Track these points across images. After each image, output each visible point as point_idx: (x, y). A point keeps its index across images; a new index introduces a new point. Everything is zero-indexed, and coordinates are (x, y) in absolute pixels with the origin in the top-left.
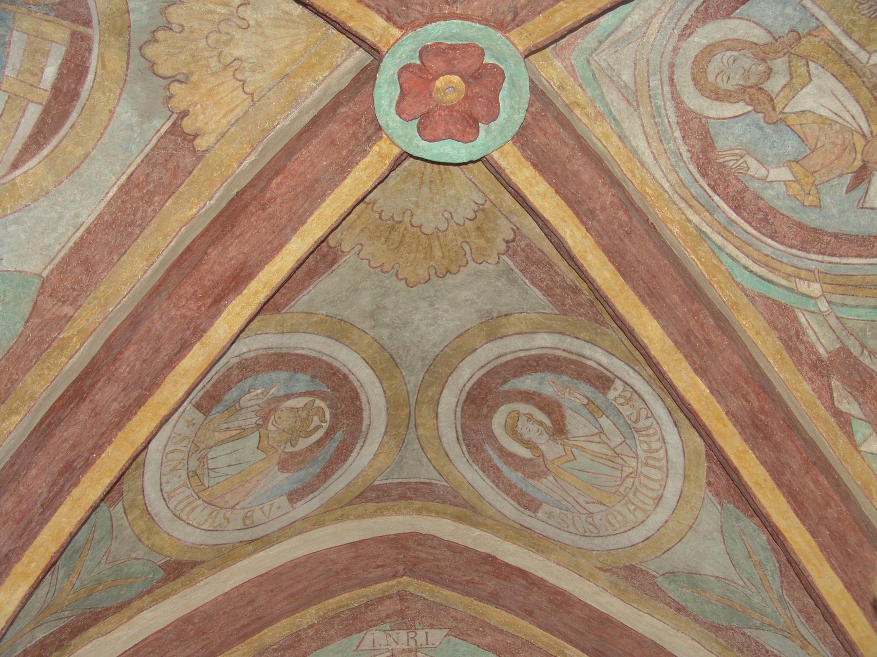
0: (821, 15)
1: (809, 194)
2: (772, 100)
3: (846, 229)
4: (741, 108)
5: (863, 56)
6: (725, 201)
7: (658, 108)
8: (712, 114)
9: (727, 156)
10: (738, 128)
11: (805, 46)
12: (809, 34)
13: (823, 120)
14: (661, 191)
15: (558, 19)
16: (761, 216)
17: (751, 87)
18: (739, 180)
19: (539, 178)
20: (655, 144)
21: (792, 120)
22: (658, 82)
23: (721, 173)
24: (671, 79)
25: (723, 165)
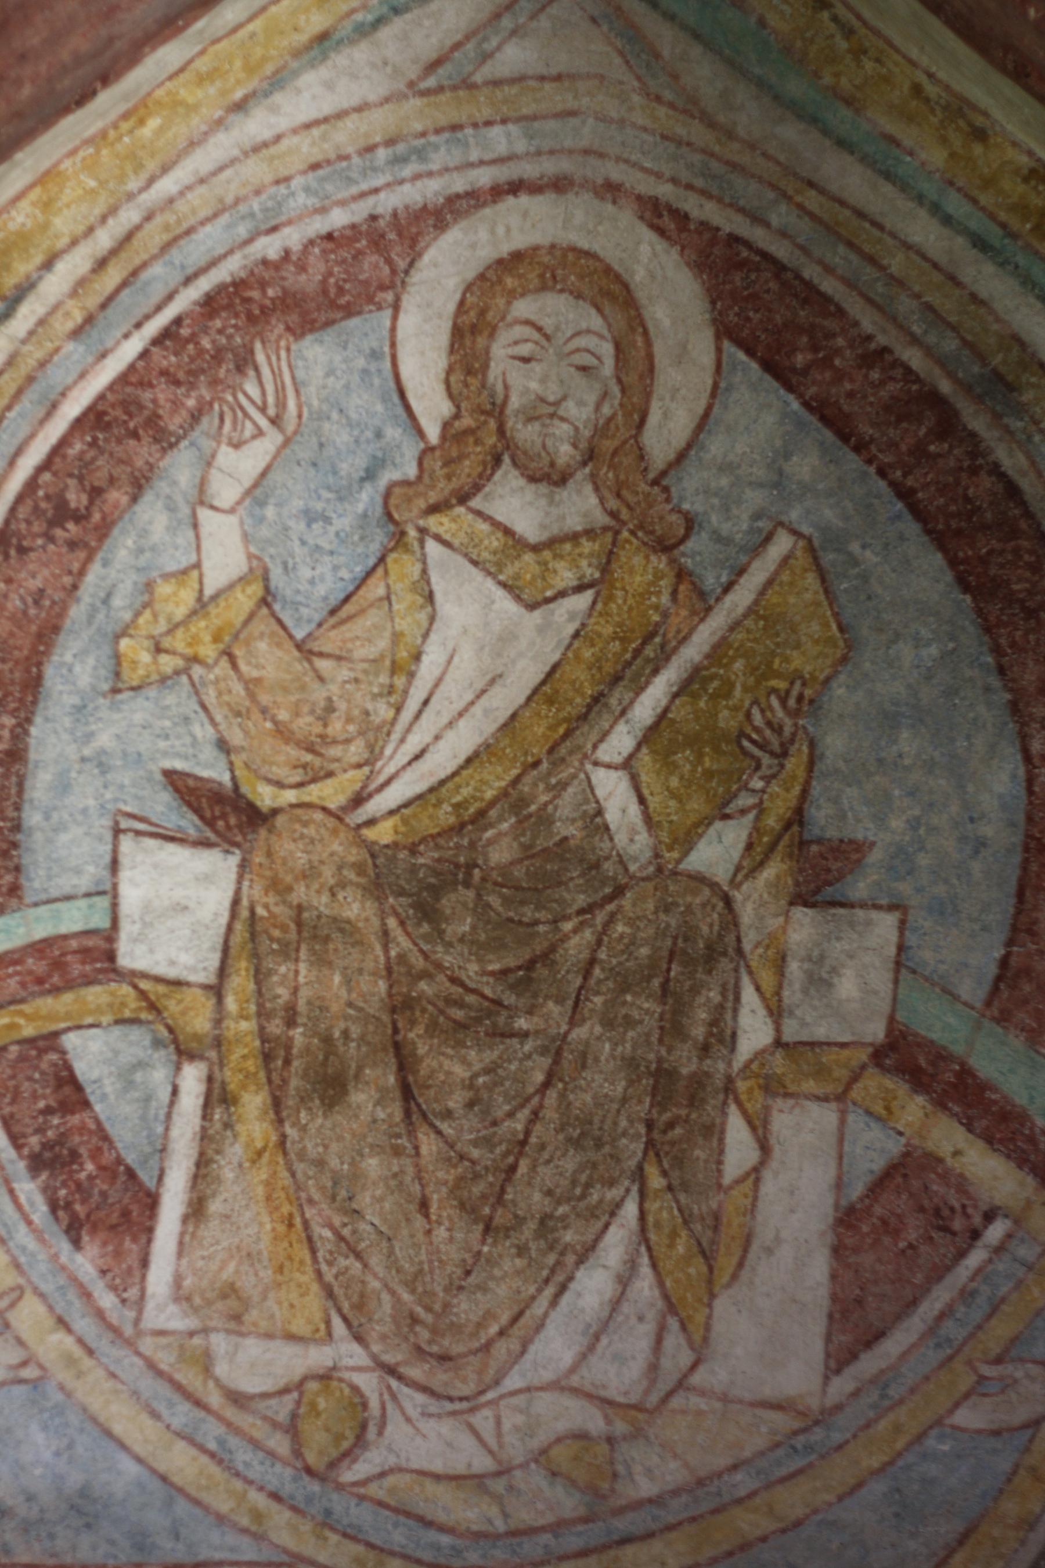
0: (742, 597)
1: (158, 650)
2: (463, 499)
3: (40, 784)
4: (432, 407)
5: (620, 742)
6: (123, 379)
7: (421, 154)
8: (408, 322)
9: (276, 375)
10: (368, 404)
11: (640, 569)
12: (681, 574)
13: (403, 665)
14: (152, 166)
16: (76, 498)
17: (501, 431)
18: (195, 417)
20: (308, 148)
21: (404, 568)
22: (502, 148)
23: (218, 357)
24: (515, 188)
25: (244, 362)
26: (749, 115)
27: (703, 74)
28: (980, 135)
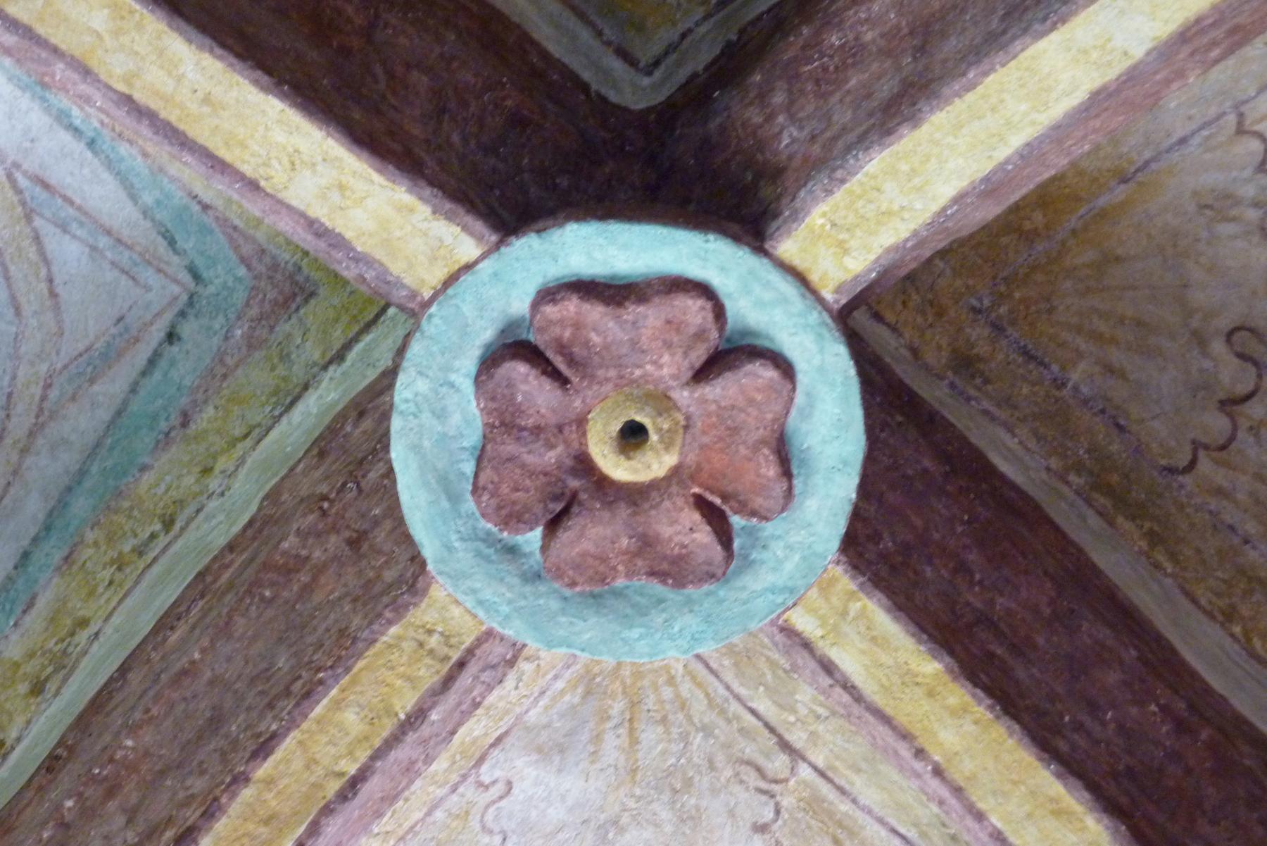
15: (351, 718)
19: (318, 211)
26: (47, 468)
27: (81, 422)
28: (38, 689)
